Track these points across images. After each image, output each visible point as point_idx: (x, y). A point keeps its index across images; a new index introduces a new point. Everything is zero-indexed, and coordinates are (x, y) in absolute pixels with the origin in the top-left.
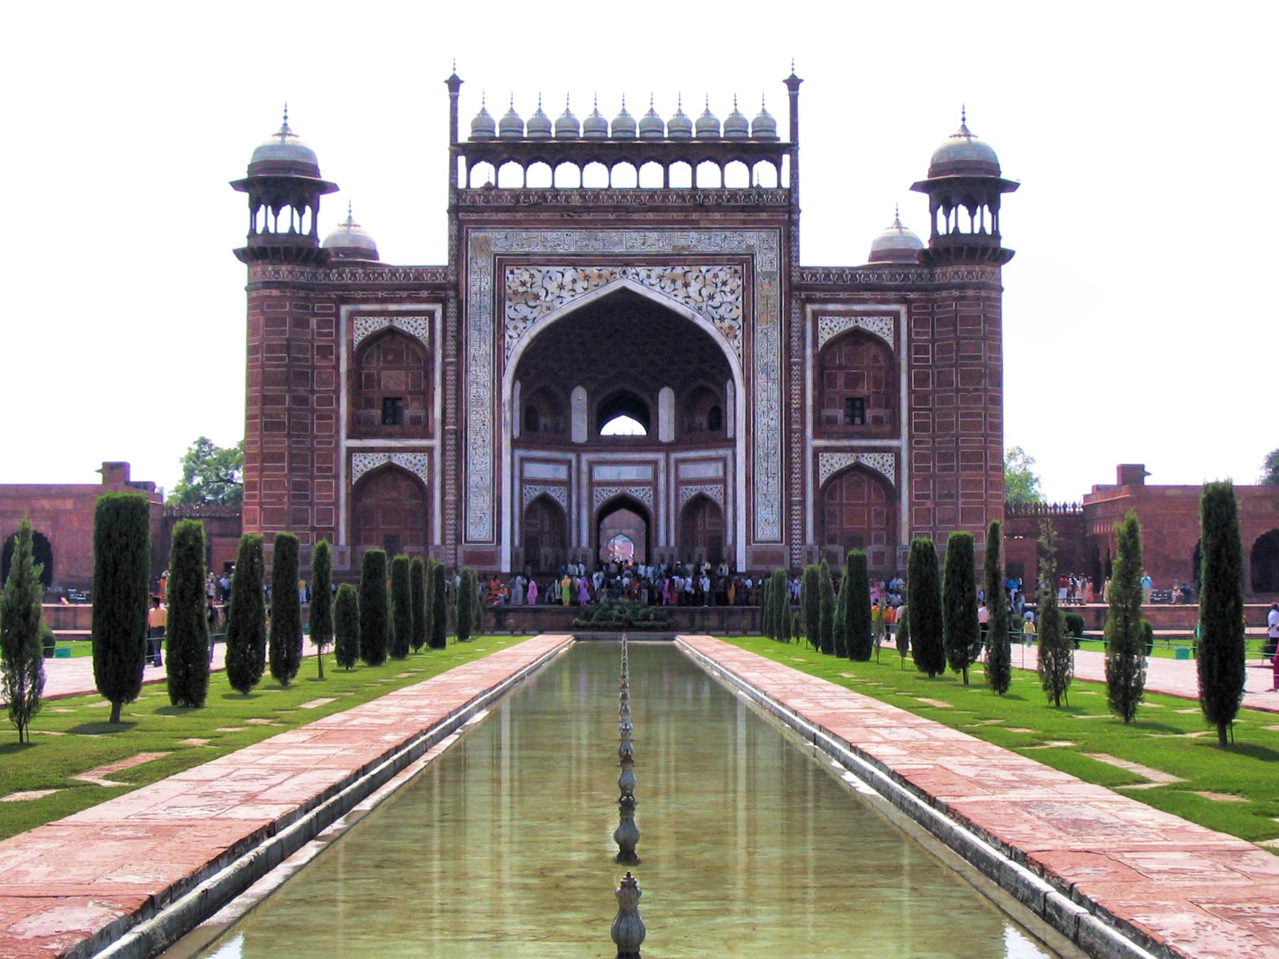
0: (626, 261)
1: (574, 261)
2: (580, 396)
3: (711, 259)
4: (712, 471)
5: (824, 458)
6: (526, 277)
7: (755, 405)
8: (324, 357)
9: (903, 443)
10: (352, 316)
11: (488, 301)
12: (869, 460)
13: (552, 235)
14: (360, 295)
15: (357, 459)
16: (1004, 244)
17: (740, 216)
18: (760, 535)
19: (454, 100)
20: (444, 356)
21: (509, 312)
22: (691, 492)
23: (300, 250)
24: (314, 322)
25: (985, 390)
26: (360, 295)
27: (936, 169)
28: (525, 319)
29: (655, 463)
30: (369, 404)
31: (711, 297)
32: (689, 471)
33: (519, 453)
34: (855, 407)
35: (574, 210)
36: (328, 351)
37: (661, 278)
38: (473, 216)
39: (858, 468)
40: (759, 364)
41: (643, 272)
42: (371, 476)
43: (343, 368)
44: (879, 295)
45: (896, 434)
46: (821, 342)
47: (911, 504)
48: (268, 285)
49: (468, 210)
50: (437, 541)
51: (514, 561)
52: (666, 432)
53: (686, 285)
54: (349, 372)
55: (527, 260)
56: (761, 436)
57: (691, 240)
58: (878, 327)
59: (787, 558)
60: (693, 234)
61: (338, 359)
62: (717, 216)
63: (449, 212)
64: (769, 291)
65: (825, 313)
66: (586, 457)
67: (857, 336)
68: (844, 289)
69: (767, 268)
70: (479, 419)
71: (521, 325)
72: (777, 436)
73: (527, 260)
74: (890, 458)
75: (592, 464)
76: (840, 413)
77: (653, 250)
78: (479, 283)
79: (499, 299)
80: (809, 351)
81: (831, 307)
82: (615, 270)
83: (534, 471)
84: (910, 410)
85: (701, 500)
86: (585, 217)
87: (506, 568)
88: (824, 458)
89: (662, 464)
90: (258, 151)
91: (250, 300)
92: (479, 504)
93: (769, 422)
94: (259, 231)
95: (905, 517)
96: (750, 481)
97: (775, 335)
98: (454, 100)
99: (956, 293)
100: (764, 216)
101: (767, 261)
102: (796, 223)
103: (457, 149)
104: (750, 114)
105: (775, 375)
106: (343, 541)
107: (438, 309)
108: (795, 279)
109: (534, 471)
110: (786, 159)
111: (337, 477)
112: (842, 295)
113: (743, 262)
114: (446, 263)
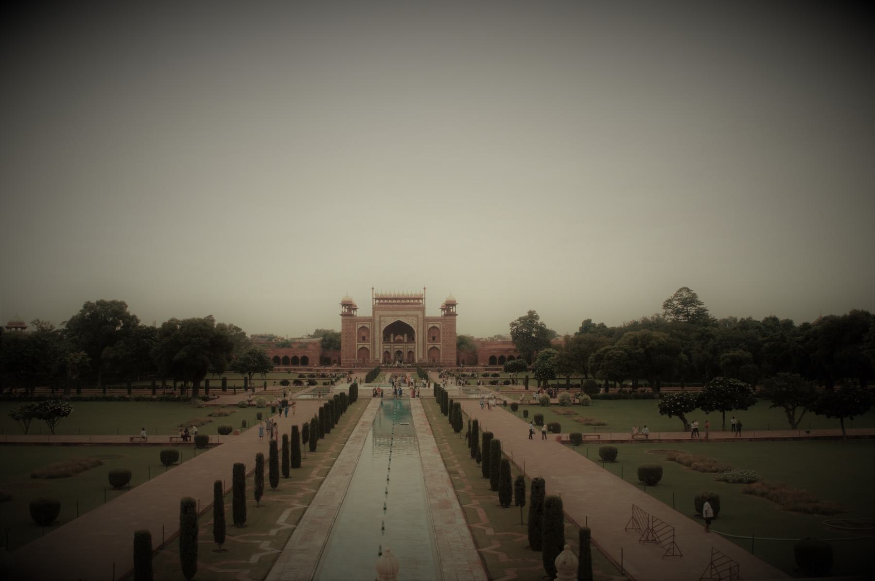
1: (392, 316)
2: (392, 335)
3: (413, 316)
7: (419, 337)
34: (434, 338)
52: (406, 340)
58: (437, 326)
64: (421, 321)
70: (377, 340)
78: (377, 319)
79: (380, 322)
85: (411, 352)
92: (377, 353)
93: (421, 340)
101: (420, 316)
104: (418, 293)
113: (417, 316)
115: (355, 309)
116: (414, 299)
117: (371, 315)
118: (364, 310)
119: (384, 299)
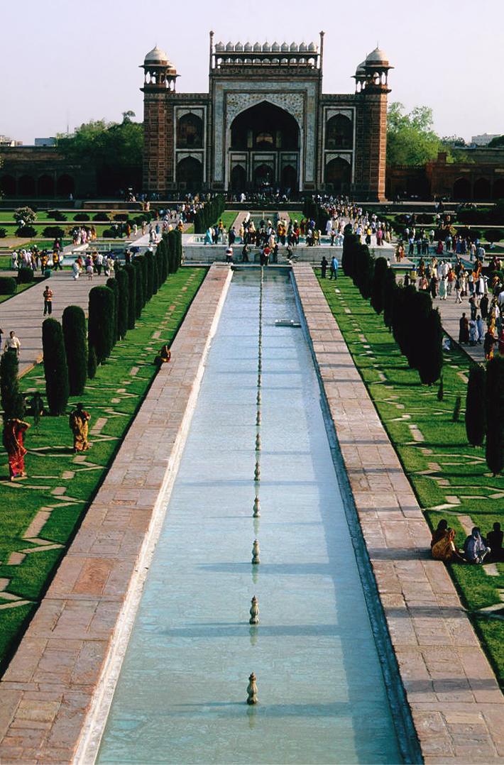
0: (266, 92)
3: (293, 92)
4: (293, 158)
5: (328, 156)
6: (234, 97)
7: (308, 140)
8: (169, 123)
9: (353, 151)
10: (178, 109)
11: (221, 105)
12: (342, 156)
13: (242, 84)
14: (180, 103)
15: (179, 155)
16: (389, 88)
17: (303, 78)
18: (307, 180)
19: (211, 39)
20: (208, 122)
21: (228, 108)
22: (286, 164)
23: (162, 88)
24: (165, 111)
25: (379, 135)
26: (180, 103)
27: (368, 62)
28: (233, 111)
29: (274, 154)
30: (183, 137)
31: (293, 104)
32: (285, 158)
33: (230, 152)
34: (339, 139)
35: (251, 76)
36: (170, 121)
37: (277, 97)
38: (217, 78)
39: (339, 159)
40: (308, 125)
41: (271, 95)
42: (184, 160)
43: (175, 126)
44: (347, 104)
45: (352, 149)
46: (328, 119)
47: (355, 171)
48: (152, 100)
49: (215, 75)
50: (205, 181)
51: (229, 188)
53: (285, 100)
54: (177, 128)
55: (234, 92)
56: (308, 148)
57: (287, 85)
58: (347, 114)
59: (315, 186)
60: (288, 84)
61: (173, 123)
62: (296, 78)
63: (209, 76)
64: (312, 102)
65: (330, 109)
66: (252, 153)
67: (340, 115)
68: (336, 101)
69: (311, 95)
71: (232, 113)
72: (313, 148)
73: (234, 92)
74: (349, 156)
75: (253, 155)
76: (334, 141)
77: (275, 89)
78: (219, 99)
79: (225, 103)
80: (324, 121)
81: (331, 107)
82: (263, 95)
83: (235, 158)
84: (356, 140)
86: (253, 78)
87: (226, 190)
88: (328, 156)
89: (277, 155)
90: (147, 56)
91: (145, 104)
92: (218, 170)
93: (310, 144)
94: (148, 82)
95: (353, 175)
96: (304, 162)
97: (313, 116)
98: (211, 39)
99: (372, 104)
100: (311, 78)
101: (311, 92)
102: (321, 80)
103: (211, 56)
104: (307, 44)
105: (313, 129)
106: (174, 181)
107: (205, 107)
108: (321, 98)
109: (235, 158)
110: (319, 57)
111: (173, 161)
112: (335, 103)
113: (304, 93)
114: (208, 92)
115: (173, 78)
116: (298, 57)
117: (204, 88)
118: (192, 79)
119: (234, 57)
